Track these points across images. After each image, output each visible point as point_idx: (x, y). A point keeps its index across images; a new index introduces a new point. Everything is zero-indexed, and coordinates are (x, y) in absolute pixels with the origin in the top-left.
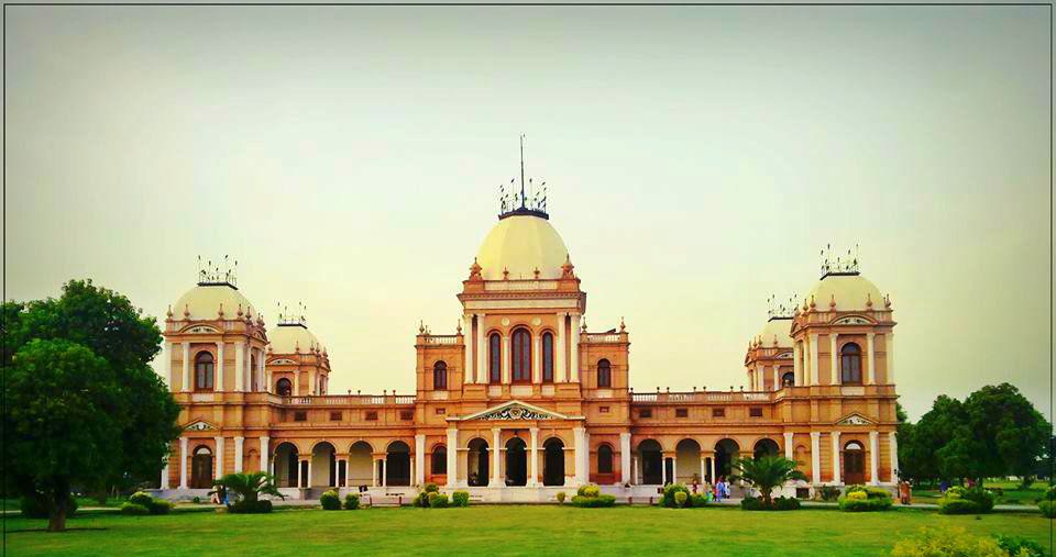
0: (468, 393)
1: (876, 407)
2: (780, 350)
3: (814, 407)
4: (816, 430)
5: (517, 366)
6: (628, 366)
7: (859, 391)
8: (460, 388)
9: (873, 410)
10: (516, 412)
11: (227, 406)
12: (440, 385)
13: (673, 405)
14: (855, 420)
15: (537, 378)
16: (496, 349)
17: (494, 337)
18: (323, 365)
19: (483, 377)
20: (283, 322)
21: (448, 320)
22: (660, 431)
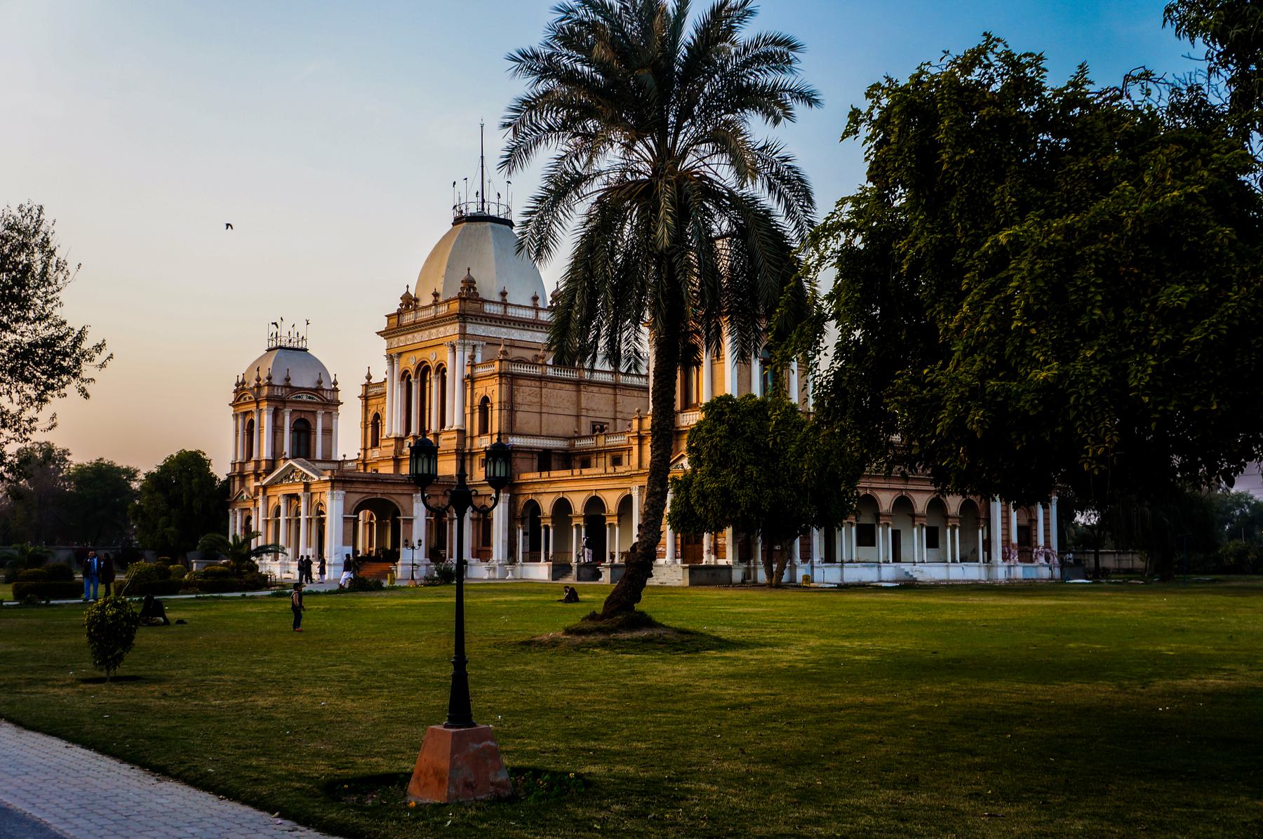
12: (375, 444)
22: (538, 488)
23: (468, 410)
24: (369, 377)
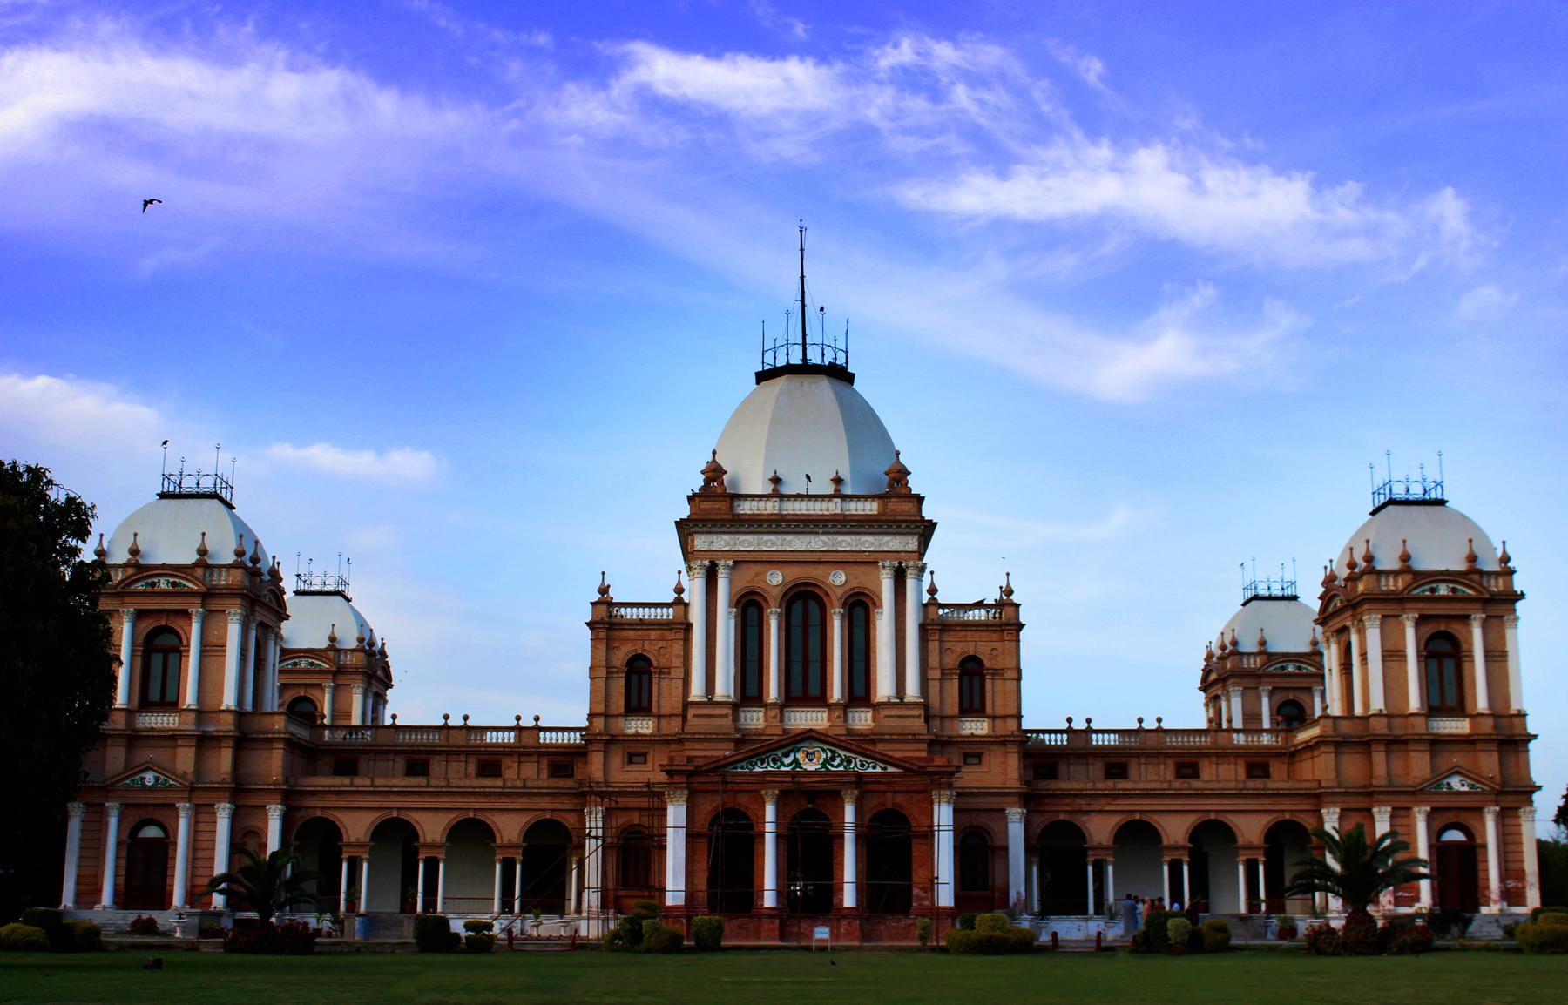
0: (696, 721)
1: (1495, 756)
2: (1270, 657)
3: (1379, 758)
4: (1385, 803)
5: (797, 669)
6: (1019, 671)
7: (1461, 726)
8: (680, 711)
9: (1489, 763)
10: (810, 756)
11: (204, 742)
12: (638, 704)
13: (1103, 753)
14: (1456, 783)
15: (836, 693)
16: (752, 633)
17: (749, 607)
18: (380, 673)
19: (725, 687)
20: (304, 587)
21: (652, 572)
22: (1082, 804)
23: (935, 674)
24: (604, 590)
